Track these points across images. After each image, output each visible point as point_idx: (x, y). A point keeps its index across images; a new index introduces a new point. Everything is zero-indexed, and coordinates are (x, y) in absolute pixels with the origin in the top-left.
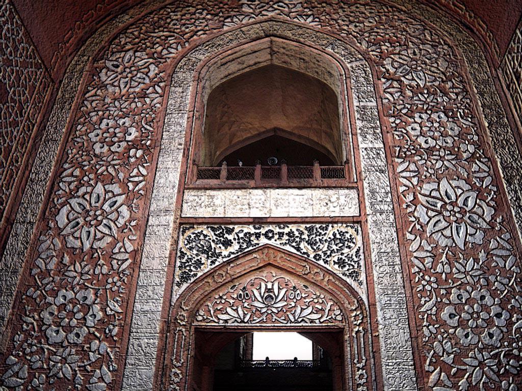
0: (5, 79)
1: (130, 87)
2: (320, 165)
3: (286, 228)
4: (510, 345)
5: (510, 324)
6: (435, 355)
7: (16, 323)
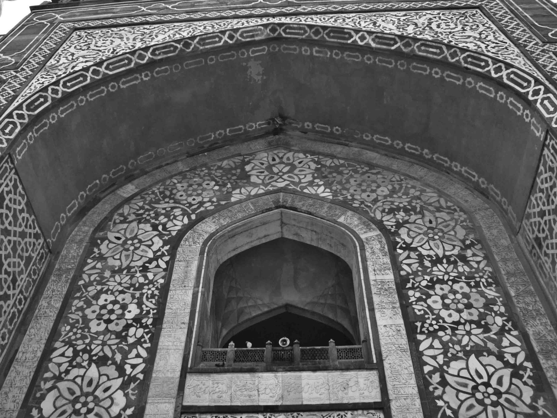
1: (132, 261)
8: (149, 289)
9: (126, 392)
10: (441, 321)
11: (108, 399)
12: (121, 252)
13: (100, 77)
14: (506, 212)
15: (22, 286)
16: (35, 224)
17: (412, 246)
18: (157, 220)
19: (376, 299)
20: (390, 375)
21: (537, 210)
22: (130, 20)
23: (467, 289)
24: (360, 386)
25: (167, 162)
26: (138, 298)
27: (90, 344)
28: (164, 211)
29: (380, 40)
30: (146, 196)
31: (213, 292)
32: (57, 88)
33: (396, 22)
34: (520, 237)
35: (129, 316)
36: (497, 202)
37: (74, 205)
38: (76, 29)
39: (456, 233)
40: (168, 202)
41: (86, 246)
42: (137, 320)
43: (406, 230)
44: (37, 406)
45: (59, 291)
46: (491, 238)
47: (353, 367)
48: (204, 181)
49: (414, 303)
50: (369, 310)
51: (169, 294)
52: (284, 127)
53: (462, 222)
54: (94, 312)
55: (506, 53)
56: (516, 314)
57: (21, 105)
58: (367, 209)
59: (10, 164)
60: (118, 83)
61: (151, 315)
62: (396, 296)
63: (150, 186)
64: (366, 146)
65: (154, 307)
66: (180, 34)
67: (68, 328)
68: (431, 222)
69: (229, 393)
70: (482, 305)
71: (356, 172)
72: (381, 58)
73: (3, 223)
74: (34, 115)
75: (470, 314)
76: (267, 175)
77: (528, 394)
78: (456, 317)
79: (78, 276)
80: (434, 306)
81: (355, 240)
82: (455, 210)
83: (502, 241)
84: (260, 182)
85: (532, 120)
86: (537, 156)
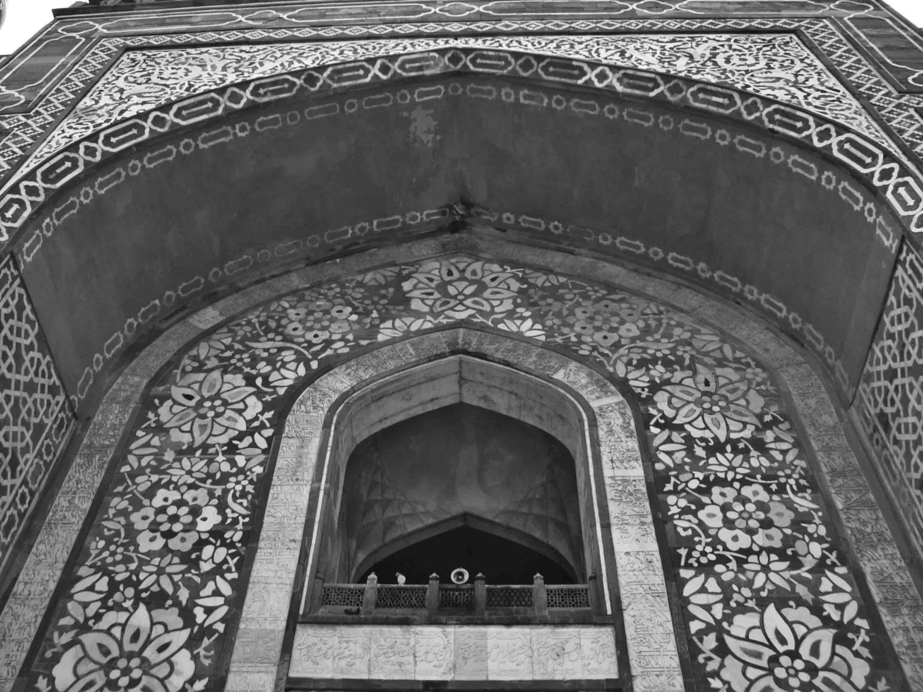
1: (211, 435)
2: (546, 583)
8: (238, 483)
9: (195, 652)
10: (720, 547)
11: (166, 665)
12: (193, 420)
13: (166, 129)
14: (832, 369)
15: (27, 473)
16: (52, 371)
17: (675, 422)
18: (253, 368)
19: (614, 509)
21: (883, 368)
22: (218, 36)
23: (764, 496)
24: (585, 652)
25: (272, 273)
26: (219, 498)
27: (137, 572)
28: (265, 355)
29: (631, 81)
30: (236, 328)
31: (344, 490)
32: (94, 145)
33: (658, 52)
34: (853, 410)
35: (203, 526)
36: (817, 352)
37: (117, 340)
38: (128, 49)
39: (748, 402)
40: (273, 340)
41: (134, 410)
42: (217, 533)
43: (667, 395)
44: (45, 672)
45: (87, 482)
46: (806, 412)
47: (571, 621)
48: (334, 305)
49: (677, 517)
50: (602, 527)
51: (271, 491)
52: (468, 220)
53: (758, 384)
54: (145, 518)
55: (839, 108)
56: (845, 540)
57: (34, 171)
58: (602, 359)
59: (12, 270)
60: (195, 140)
61: (240, 527)
62: (647, 504)
63: (244, 313)
64: (603, 256)
65: (245, 512)
66: (299, 62)
67: (102, 544)
68: (707, 383)
70: (788, 523)
71: (586, 297)
72: (631, 110)
74: (53, 190)
75: (769, 537)
76: (439, 299)
77: (861, 671)
78: (745, 541)
79: (120, 458)
80: (708, 522)
81: (581, 409)
82: (748, 365)
83: (824, 418)
84: (427, 309)
85: (878, 220)
86: (885, 279)
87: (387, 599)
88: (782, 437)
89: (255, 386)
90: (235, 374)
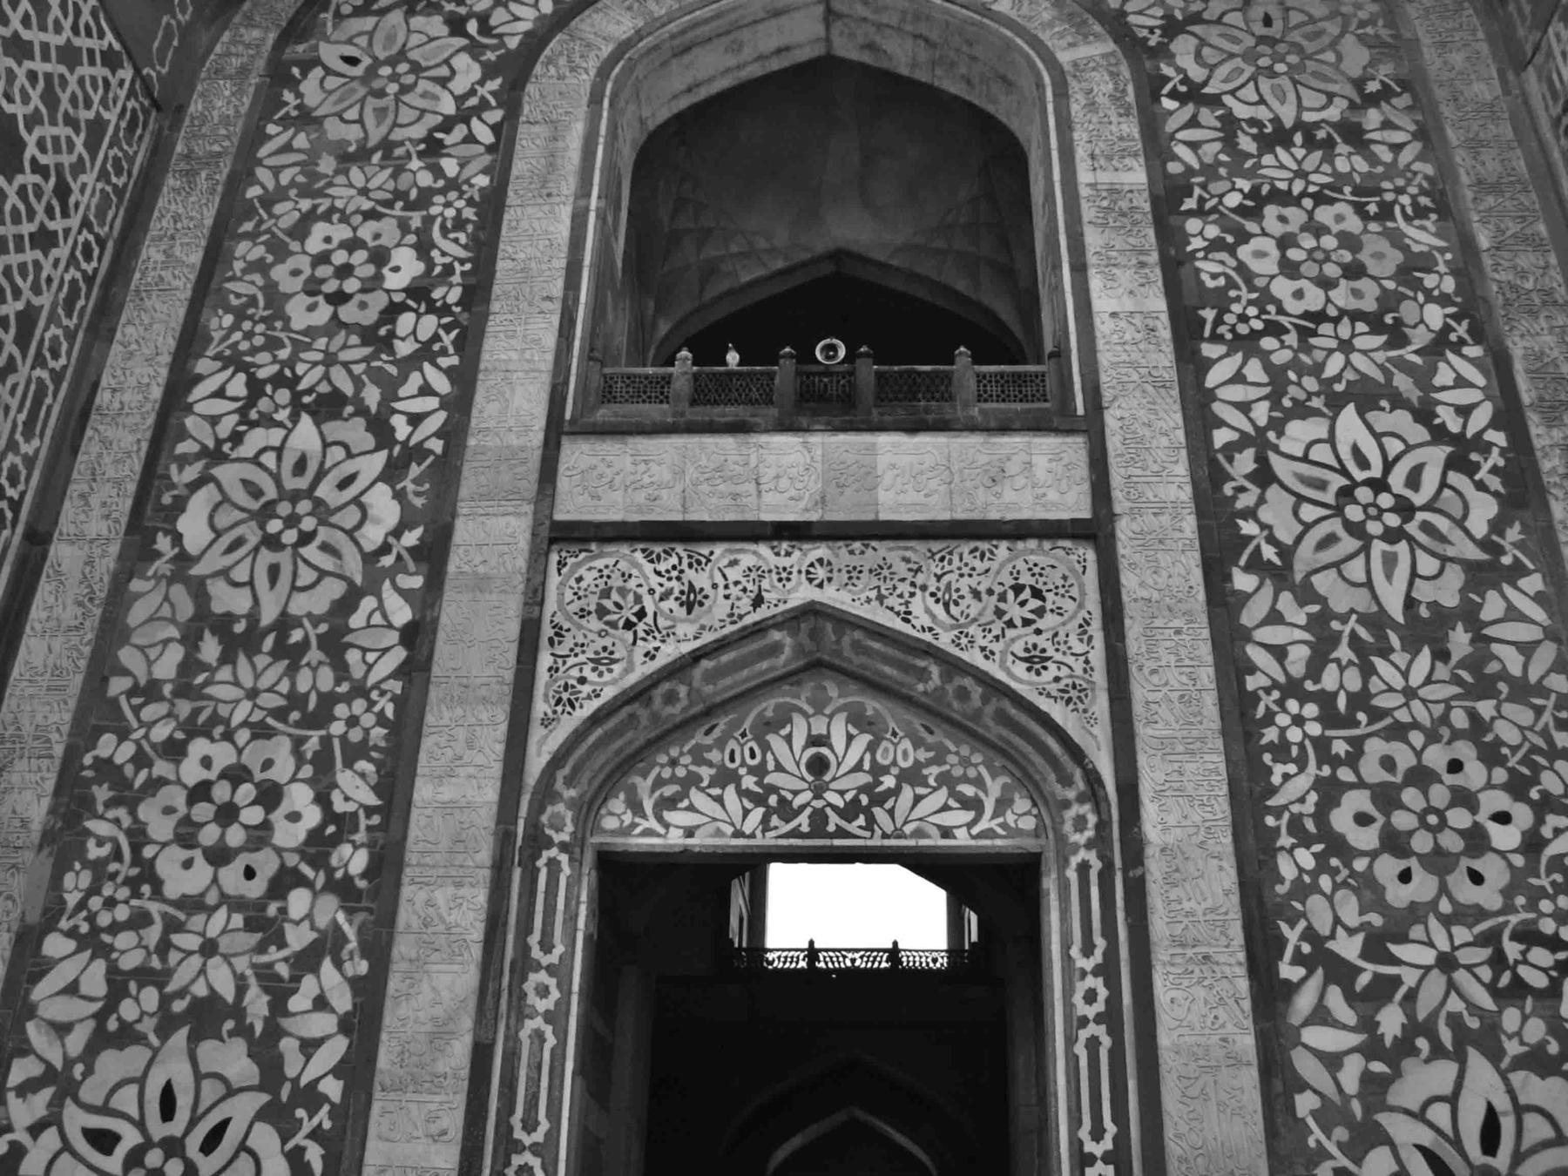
0: (10, 100)
1: (395, 125)
3: (869, 552)
4: (1532, 905)
5: (1533, 844)
6: (1310, 935)
7: (63, 838)
8: (448, 205)
10: (1271, 308)
11: (353, 507)
12: (362, 101)
15: (88, 207)
17: (1206, 90)
20: (1121, 449)
23: (1353, 224)
24: (1037, 474)
26: (417, 232)
27: (291, 363)
41: (258, 87)
42: (418, 292)
43: (1194, 41)
47: (1017, 425)
49: (1200, 255)
50: (1073, 269)
51: (506, 217)
53: (1362, 24)
54: (296, 273)
56: (1486, 301)
61: (456, 279)
62: (1151, 232)
65: (463, 254)
67: (228, 320)
68: (1268, 21)
69: (679, 488)
70: (1390, 268)
73: (5, 22)
75: (1357, 294)
78: (1314, 299)
80: (1256, 266)
81: (1041, 65)
87: (709, 390)
88: (1397, 121)
89: (466, 35)
90: (429, 15)
